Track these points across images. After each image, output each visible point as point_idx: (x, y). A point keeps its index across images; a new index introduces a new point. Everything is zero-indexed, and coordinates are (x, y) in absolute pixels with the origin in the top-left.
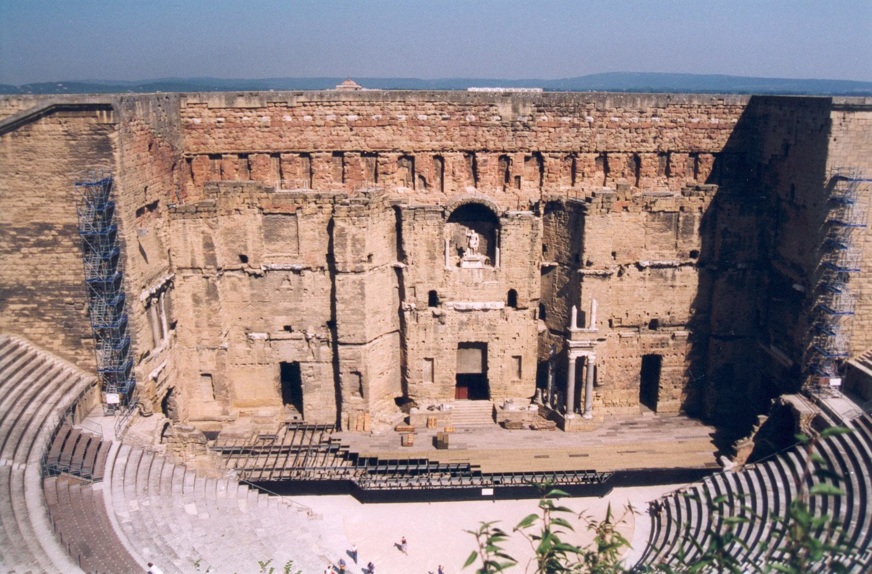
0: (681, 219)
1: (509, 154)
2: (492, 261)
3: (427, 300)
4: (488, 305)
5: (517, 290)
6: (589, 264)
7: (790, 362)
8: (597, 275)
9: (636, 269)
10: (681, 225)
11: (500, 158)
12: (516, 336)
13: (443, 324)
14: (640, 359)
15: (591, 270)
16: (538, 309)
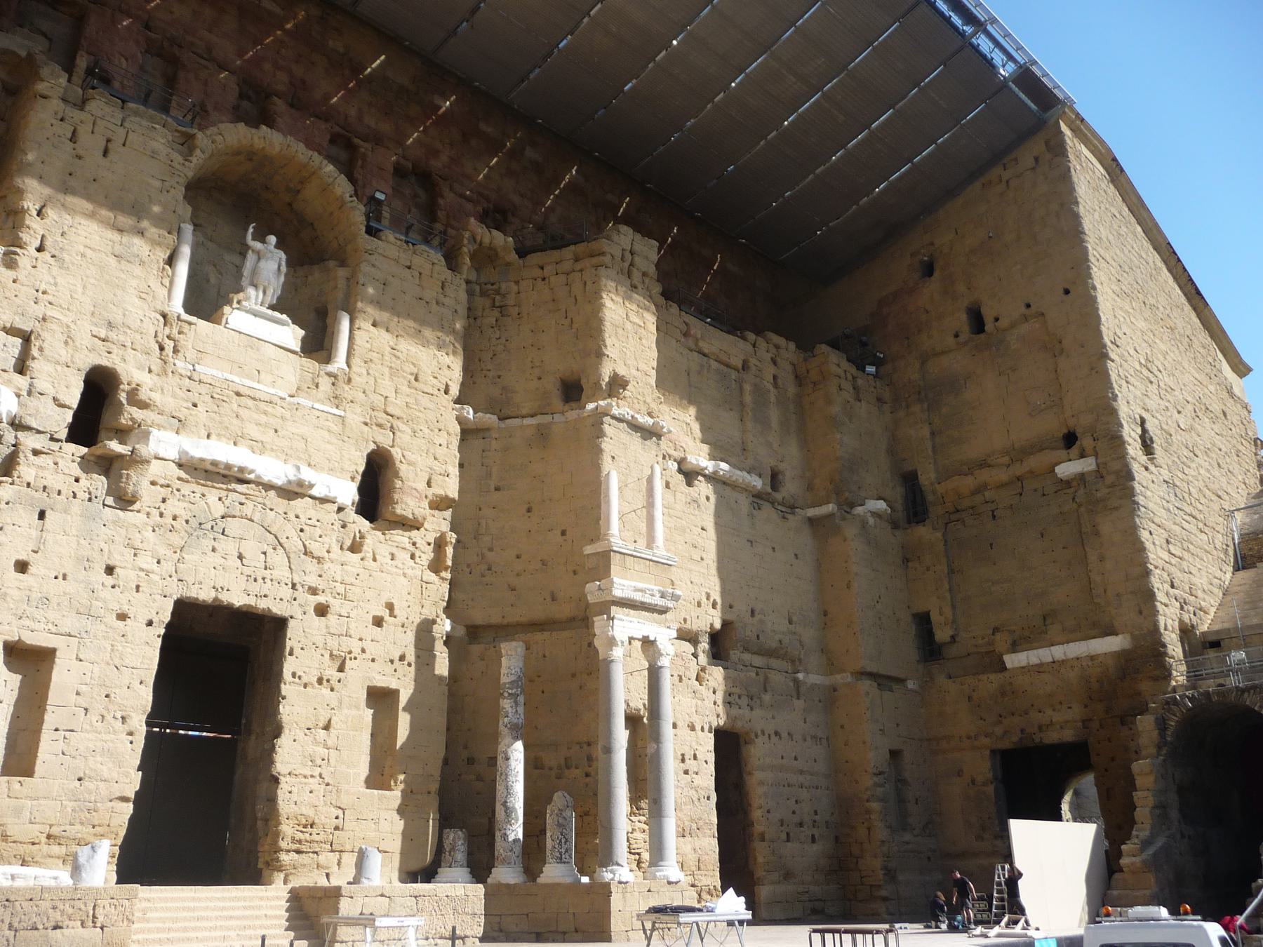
0: (747, 387)
1: (357, 141)
2: (318, 344)
3: (73, 396)
4: (307, 475)
5: (396, 453)
6: (618, 385)
7: (1113, 644)
8: (635, 427)
9: (681, 477)
10: (748, 399)
11: (334, 140)
12: (385, 613)
13: (125, 501)
14: (712, 735)
15: (620, 408)
16: (452, 537)
